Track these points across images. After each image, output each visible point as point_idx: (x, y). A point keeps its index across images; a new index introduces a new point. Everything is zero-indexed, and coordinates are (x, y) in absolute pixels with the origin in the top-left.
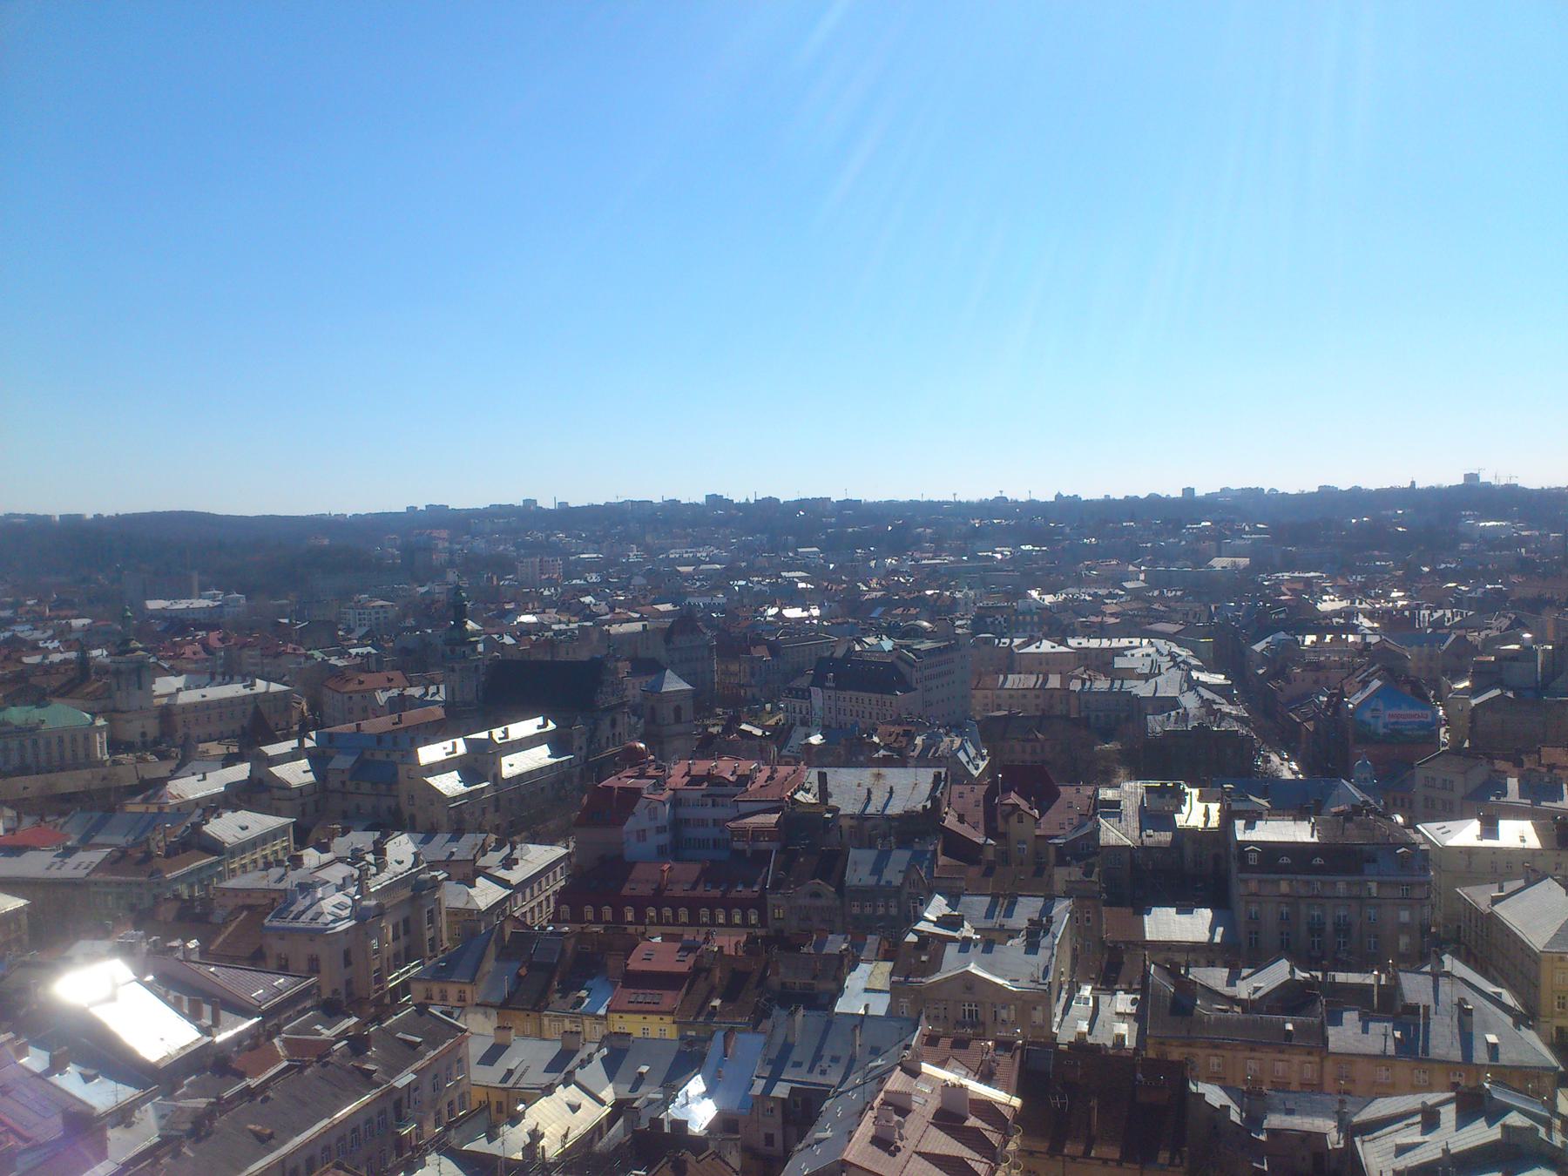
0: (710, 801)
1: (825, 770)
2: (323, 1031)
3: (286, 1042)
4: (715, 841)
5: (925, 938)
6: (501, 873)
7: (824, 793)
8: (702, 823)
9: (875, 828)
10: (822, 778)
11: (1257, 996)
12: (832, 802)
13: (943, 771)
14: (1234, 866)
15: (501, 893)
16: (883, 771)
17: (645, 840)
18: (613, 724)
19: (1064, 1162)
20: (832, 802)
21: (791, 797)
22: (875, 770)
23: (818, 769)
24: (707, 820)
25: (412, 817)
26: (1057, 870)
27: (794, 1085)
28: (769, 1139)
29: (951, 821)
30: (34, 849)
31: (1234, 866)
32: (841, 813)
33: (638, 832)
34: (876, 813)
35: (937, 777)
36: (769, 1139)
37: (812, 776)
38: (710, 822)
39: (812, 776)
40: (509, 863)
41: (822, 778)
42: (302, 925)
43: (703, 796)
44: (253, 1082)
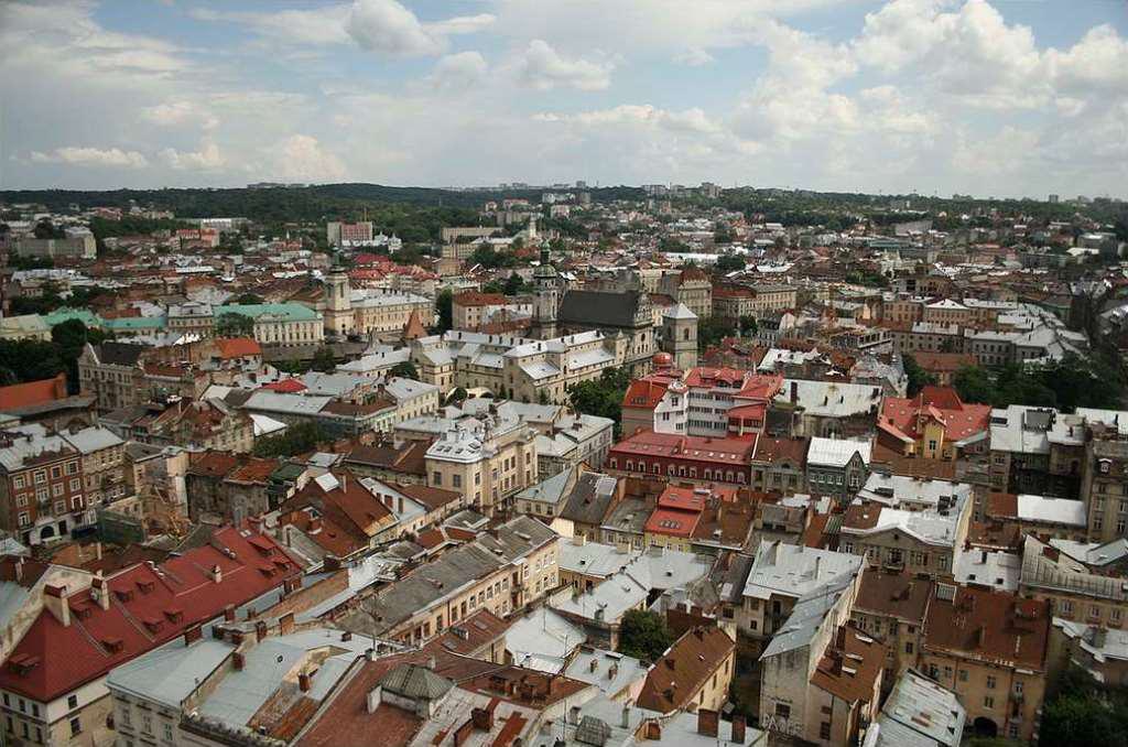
1: (796, 381)
2: (469, 525)
3: (446, 528)
5: (866, 503)
6: (572, 433)
7: (794, 397)
10: (794, 386)
11: (1101, 563)
12: (799, 403)
13: (880, 388)
14: (1089, 472)
15: (570, 444)
16: (837, 384)
18: (643, 338)
19: (957, 661)
20: (799, 403)
21: (771, 398)
22: (831, 384)
25: (511, 391)
26: (958, 463)
27: (775, 592)
28: (754, 625)
29: (884, 425)
30: (289, 393)
31: (1089, 472)
32: (806, 412)
35: (876, 391)
36: (754, 625)
37: (787, 384)
39: (787, 384)
40: (576, 427)
41: (794, 386)
44: (429, 552)
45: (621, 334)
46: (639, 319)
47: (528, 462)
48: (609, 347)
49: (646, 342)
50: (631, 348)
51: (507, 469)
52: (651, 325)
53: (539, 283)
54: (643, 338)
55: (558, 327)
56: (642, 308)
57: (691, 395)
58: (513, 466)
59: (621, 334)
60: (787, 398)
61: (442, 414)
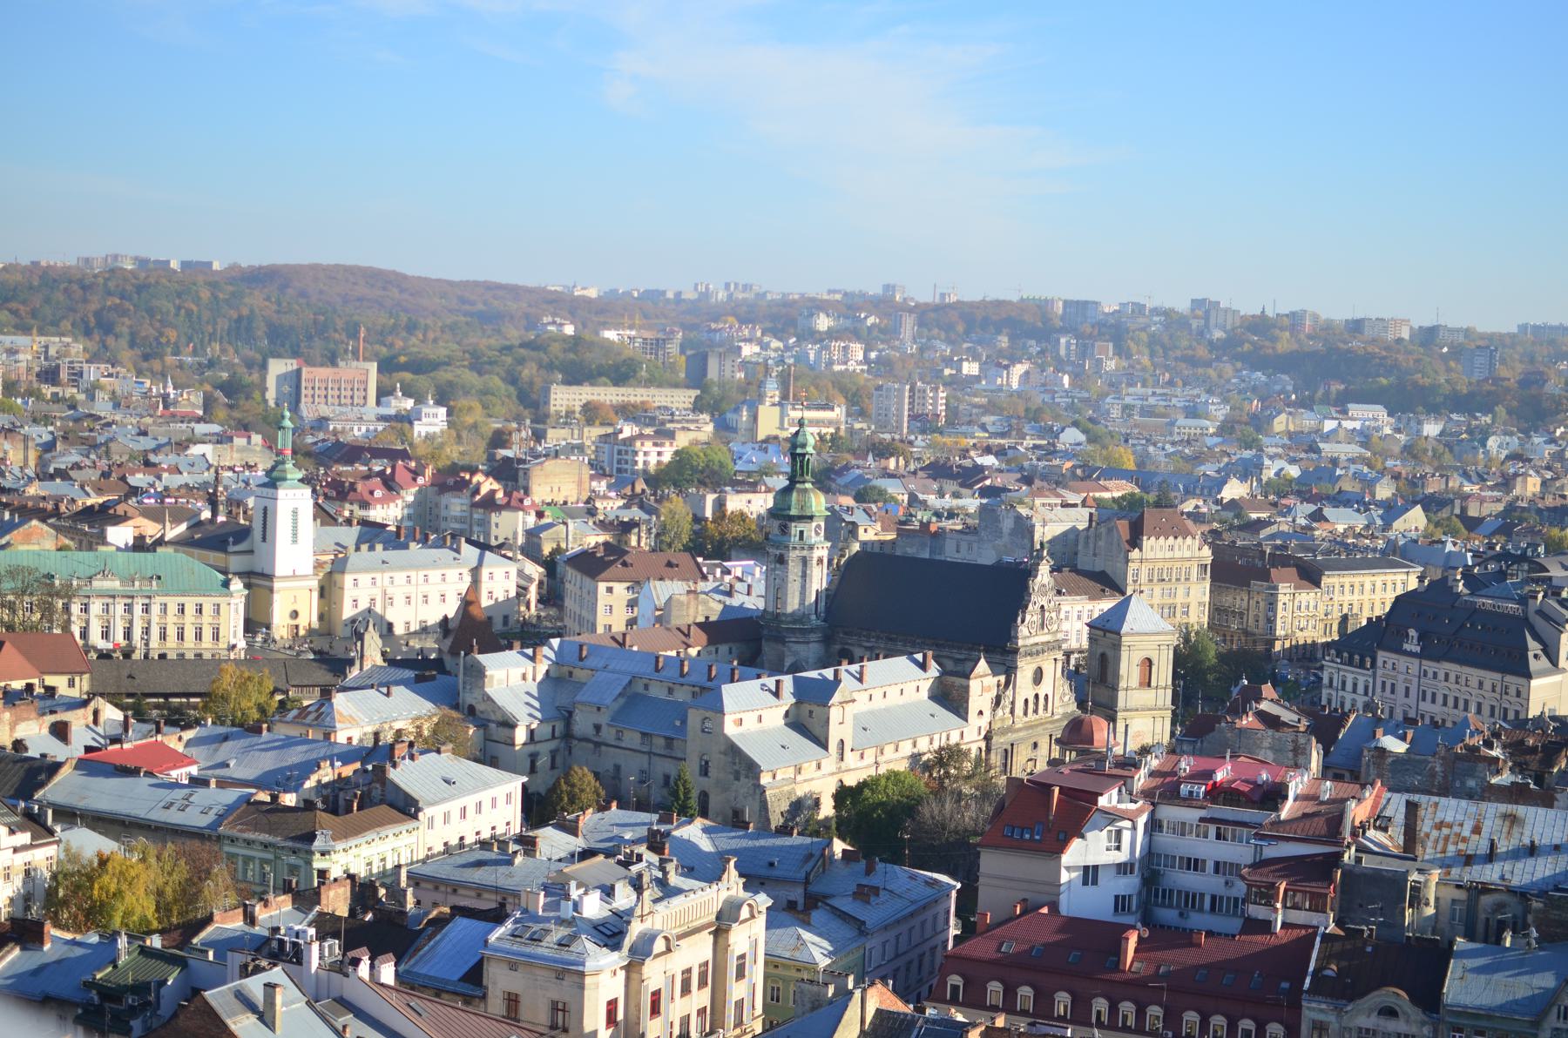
0: (1212, 829)
1: (1416, 798)
4: (1213, 898)
8: (1195, 864)
9: (1500, 907)
16: (1520, 810)
17: (1095, 882)
18: (1038, 676)
22: (1504, 808)
23: (1406, 796)
24: (1204, 861)
25: (704, 797)
33: (1086, 868)
34: (1499, 882)
37: (1396, 806)
38: (1210, 866)
40: (864, 894)
41: (1412, 808)
42: (546, 952)
43: (1202, 820)
45: (982, 666)
46: (1027, 633)
47: (741, 974)
48: (950, 697)
49: (1045, 688)
50: (1006, 702)
51: (686, 990)
52: (1056, 645)
53: (784, 530)
54: (1038, 676)
55: (827, 640)
56: (1037, 600)
57: (1154, 826)
58: (702, 983)
59: (982, 666)
60: (1390, 839)
61: (528, 844)
